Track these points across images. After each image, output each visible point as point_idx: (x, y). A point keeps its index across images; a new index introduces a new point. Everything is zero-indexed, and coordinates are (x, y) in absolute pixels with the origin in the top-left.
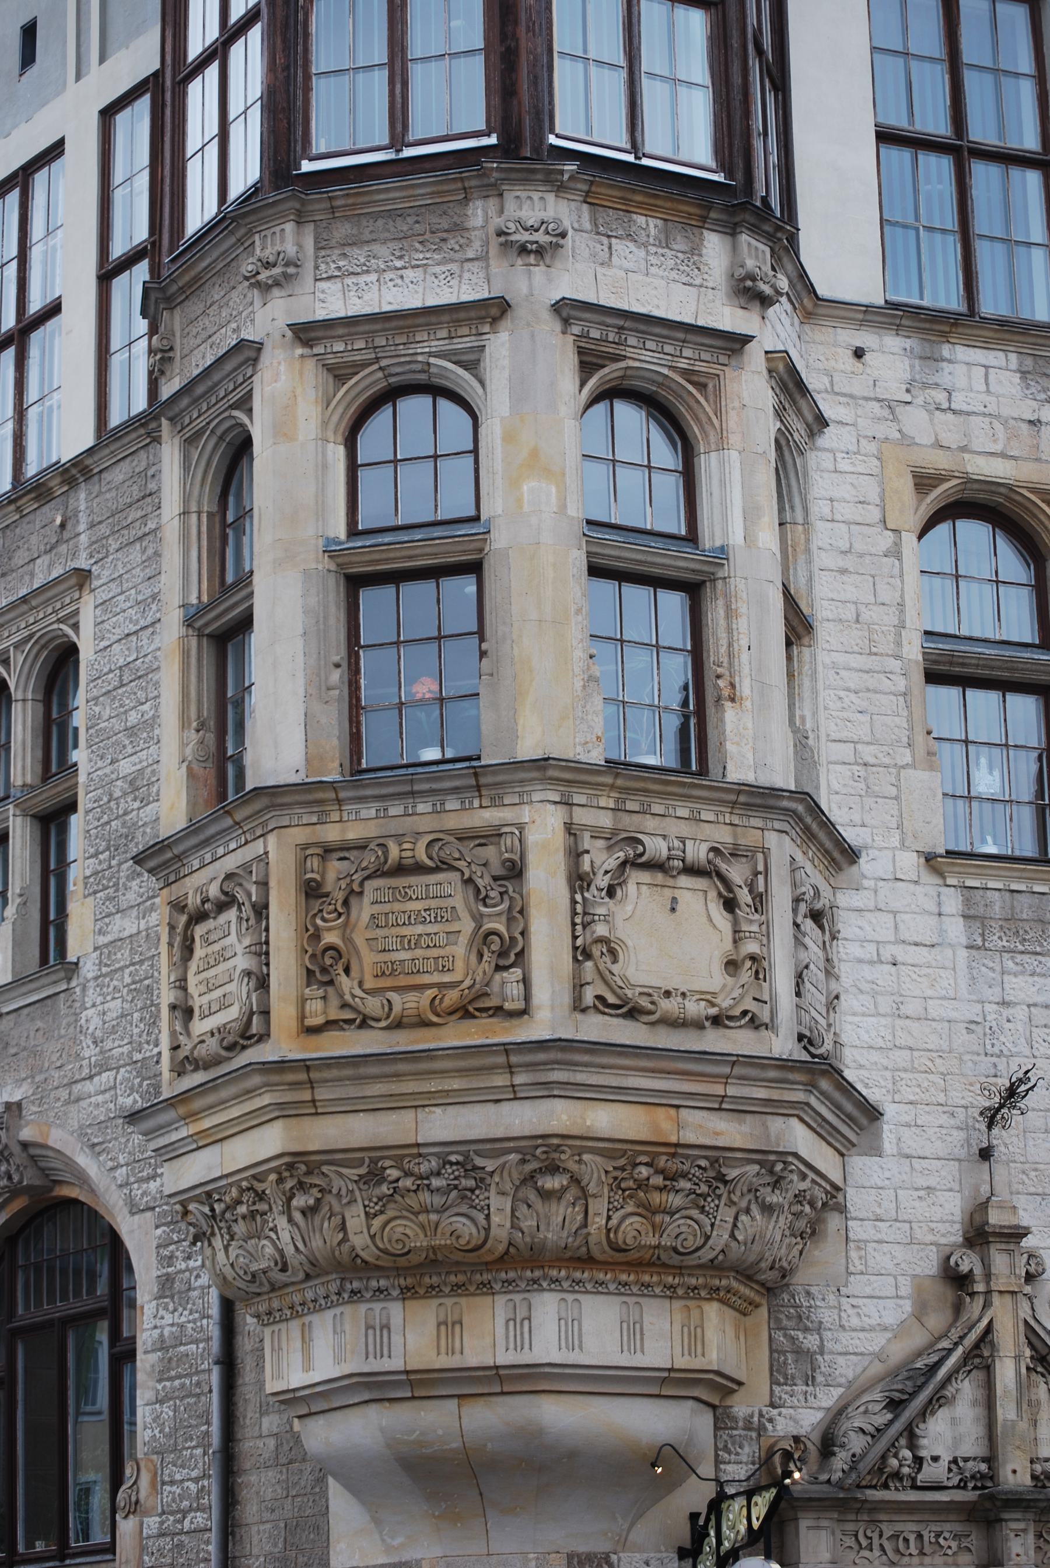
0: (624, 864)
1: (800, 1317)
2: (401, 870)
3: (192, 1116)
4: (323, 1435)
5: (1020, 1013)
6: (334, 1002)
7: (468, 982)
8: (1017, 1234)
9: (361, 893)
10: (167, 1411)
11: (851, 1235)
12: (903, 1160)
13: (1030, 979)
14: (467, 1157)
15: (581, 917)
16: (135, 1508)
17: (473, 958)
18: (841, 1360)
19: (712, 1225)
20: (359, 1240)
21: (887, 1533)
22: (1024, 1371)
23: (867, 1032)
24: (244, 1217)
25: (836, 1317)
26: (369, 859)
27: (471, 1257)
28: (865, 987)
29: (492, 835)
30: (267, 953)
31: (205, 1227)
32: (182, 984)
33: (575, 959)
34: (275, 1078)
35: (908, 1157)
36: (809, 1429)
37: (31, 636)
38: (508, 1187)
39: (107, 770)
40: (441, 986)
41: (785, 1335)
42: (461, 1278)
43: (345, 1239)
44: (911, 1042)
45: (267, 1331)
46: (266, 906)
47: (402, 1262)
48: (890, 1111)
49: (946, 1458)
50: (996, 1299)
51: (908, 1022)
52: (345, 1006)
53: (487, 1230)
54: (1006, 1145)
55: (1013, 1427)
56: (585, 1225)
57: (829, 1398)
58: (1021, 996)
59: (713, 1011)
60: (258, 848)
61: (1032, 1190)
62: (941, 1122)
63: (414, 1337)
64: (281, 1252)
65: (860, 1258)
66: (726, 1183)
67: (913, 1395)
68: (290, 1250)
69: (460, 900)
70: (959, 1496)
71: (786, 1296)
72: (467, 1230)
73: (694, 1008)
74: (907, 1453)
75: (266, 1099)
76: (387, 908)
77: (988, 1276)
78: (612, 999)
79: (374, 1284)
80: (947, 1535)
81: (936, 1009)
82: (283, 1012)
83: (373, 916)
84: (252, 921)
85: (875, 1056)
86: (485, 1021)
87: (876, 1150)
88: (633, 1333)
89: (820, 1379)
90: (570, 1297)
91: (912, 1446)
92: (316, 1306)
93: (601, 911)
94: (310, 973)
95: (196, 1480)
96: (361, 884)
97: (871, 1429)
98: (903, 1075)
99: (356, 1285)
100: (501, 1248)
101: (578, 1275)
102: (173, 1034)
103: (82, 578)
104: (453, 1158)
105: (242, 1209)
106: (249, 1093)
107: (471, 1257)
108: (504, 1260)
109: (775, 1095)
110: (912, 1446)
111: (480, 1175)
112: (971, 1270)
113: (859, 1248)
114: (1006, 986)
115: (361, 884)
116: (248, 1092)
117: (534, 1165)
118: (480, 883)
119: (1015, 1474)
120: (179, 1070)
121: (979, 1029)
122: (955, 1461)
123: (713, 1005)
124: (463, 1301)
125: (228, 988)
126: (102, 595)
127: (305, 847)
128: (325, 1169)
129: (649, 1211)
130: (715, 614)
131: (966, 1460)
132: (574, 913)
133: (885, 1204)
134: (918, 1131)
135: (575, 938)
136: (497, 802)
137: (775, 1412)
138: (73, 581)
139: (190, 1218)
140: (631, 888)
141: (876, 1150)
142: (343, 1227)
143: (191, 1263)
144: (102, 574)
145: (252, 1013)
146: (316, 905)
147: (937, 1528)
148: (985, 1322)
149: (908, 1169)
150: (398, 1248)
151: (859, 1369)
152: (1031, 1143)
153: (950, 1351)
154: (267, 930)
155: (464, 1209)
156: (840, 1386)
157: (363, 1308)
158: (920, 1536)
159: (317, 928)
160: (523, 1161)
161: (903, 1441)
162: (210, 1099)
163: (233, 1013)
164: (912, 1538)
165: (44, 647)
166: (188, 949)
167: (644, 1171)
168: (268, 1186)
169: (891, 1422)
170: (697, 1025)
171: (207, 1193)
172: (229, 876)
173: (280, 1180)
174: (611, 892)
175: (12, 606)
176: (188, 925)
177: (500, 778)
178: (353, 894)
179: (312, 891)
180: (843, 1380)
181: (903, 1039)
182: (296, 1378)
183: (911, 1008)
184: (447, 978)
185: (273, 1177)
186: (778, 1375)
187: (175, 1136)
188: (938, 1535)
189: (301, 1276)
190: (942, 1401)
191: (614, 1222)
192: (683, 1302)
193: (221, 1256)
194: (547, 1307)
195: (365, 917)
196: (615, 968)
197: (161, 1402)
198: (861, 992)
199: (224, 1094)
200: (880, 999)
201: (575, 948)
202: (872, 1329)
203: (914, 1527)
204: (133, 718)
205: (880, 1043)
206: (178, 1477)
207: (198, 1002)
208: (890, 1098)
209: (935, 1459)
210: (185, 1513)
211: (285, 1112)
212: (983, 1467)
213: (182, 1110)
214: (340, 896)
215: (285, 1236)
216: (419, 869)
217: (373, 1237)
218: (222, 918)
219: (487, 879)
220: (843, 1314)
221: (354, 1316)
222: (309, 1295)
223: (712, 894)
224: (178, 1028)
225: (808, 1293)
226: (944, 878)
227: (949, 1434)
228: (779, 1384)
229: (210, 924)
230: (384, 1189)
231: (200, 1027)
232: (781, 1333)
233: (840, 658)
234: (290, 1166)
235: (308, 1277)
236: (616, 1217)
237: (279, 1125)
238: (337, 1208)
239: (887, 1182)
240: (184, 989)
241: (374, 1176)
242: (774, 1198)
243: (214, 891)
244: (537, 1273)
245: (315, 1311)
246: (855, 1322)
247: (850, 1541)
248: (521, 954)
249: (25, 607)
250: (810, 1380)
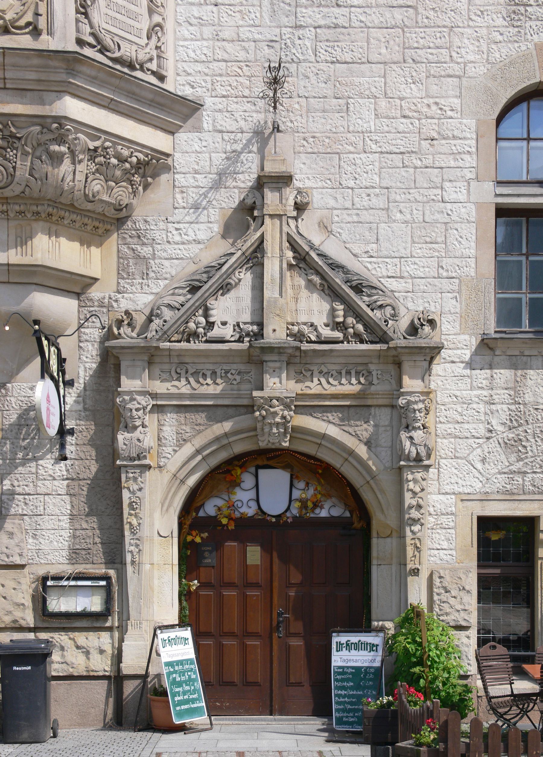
1: (139, 237)
5: (310, 33)
11: (176, 183)
12: (216, 134)
13: (316, 9)
18: (166, 263)
19: (14, 168)
21: (191, 371)
22: (285, 266)
23: (194, 51)
25: (164, 236)
28: (194, 21)
35: (221, 132)
36: (143, 306)
41: (129, 248)
44: (226, 57)
48: (209, 102)
49: (232, 322)
50: (267, 220)
51: (225, 44)
54: (291, 121)
55: (275, 302)
57: (158, 286)
58: (310, 21)
61: (310, 150)
62: (245, 108)
65: (183, 198)
71: (129, 223)
74: (202, 320)
80: (233, 372)
81: (245, 33)
85: (199, 67)
87: (198, 129)
89: (152, 275)
91: (206, 315)
97: (177, 305)
98: (219, 78)
109: (43, 77)
110: (206, 315)
112: (254, 203)
113: (182, 192)
114: (299, 15)
119: (276, 333)
121: (277, 46)
133: (202, 163)
134: (228, 115)
137: (120, 296)
141: (198, 129)
149: (220, 140)
151: (179, 269)
152: (311, 119)
156: (166, 279)
161: (201, 312)
180: (168, 276)
181: (220, 55)
183: (227, 34)
186: (123, 272)
188: (227, 372)
190: (229, 286)
192: (16, 222)
198: (191, 24)
200: (204, 29)
202: (189, 242)
203: (211, 367)
205: (204, 58)
208: (209, 94)
209: (224, 324)
212: (255, 328)
220: (169, 234)
225: (146, 221)
228: (123, 278)
232: (125, 247)
239: (204, 149)
246: (177, 238)
250: (145, 275)
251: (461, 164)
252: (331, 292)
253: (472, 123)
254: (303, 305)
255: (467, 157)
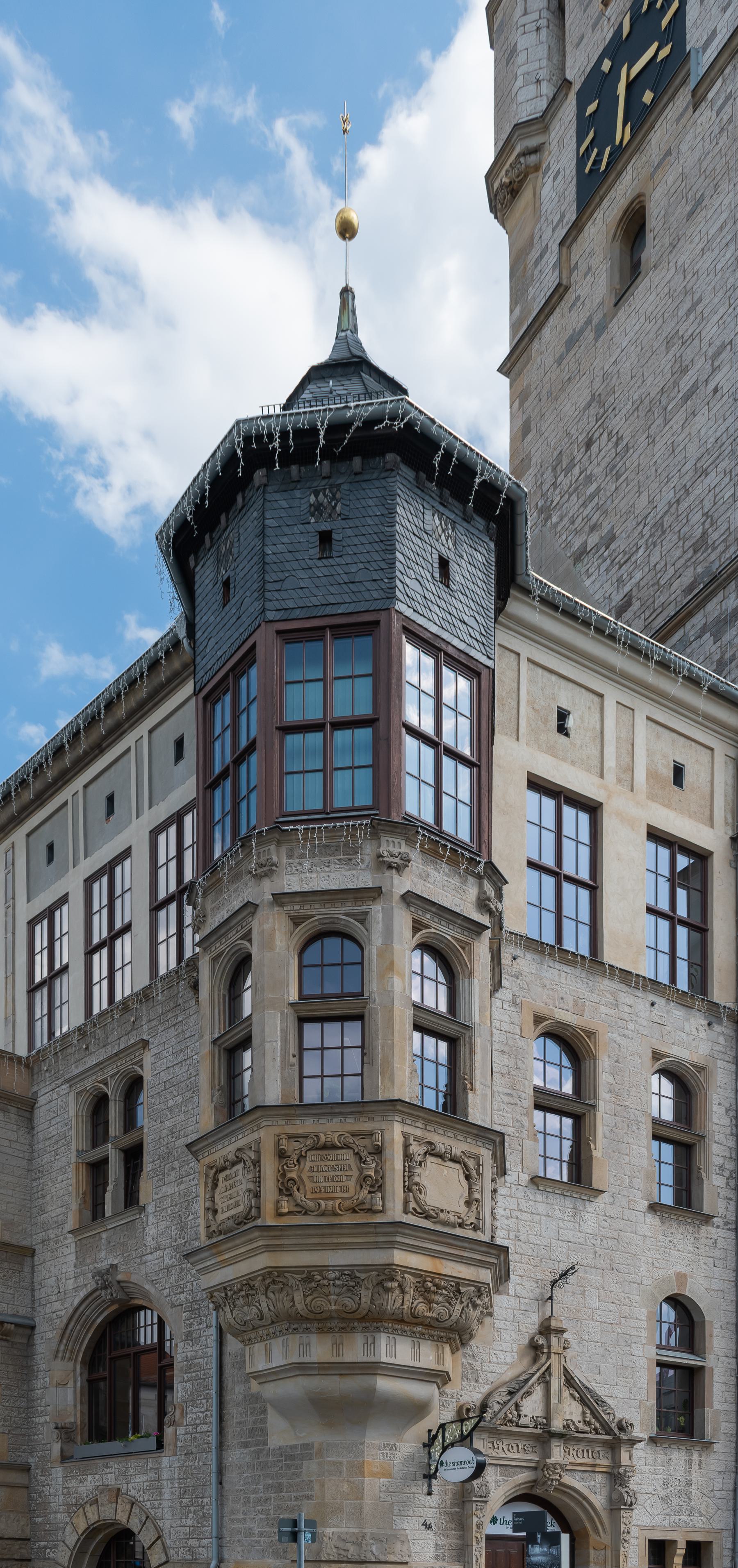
0: (426, 1153)
2: (325, 1147)
3: (220, 1253)
4: (271, 1390)
6: (292, 1203)
7: (356, 1197)
8: (561, 1331)
9: (305, 1157)
10: (189, 1385)
14: (352, 1271)
15: (409, 1173)
16: (173, 1423)
17: (358, 1187)
20: (300, 1307)
24: (243, 1297)
26: (309, 1142)
27: (350, 1316)
29: (371, 1134)
30: (259, 1182)
31: (221, 1302)
32: (212, 1199)
33: (404, 1191)
34: (265, 1234)
37: (118, 1072)
38: (371, 1286)
39: (159, 1126)
40: (343, 1198)
42: (344, 1325)
43: (294, 1305)
45: (247, 1348)
46: (259, 1161)
47: (318, 1316)
52: (297, 1205)
53: (359, 1304)
56: (402, 1305)
59: (460, 1221)
60: (255, 1136)
63: (319, 1350)
64: (261, 1311)
66: (460, 1293)
67: (519, 1390)
68: (266, 1310)
69: (352, 1161)
70: (534, 1431)
72: (350, 1304)
73: (452, 1218)
75: (260, 1243)
76: (317, 1163)
77: (549, 1347)
78: (419, 1210)
79: (304, 1326)
82: (268, 1207)
83: (311, 1167)
84: (252, 1168)
86: (362, 1214)
88: (416, 1355)
90: (391, 1336)
92: (275, 1336)
93: (417, 1171)
94: (280, 1190)
95: (203, 1412)
96: (306, 1153)
99: (296, 1326)
100: (365, 1312)
101: (396, 1326)
102: (207, 1220)
103: (145, 1044)
104: (346, 1272)
105: (243, 1293)
106: (251, 1241)
107: (350, 1316)
108: (363, 1319)
111: (358, 1280)
115: (306, 1153)
116: (251, 1240)
117: (383, 1277)
118: (362, 1154)
119: (557, 1425)
120: (209, 1236)
122: (533, 1417)
123: (459, 1218)
124: (344, 1335)
125: (237, 1199)
126: (154, 1051)
127: (278, 1135)
128: (286, 1274)
129: (429, 1302)
130: (463, 1052)
131: (537, 1417)
132: (404, 1171)
135: (404, 1182)
136: (371, 1119)
138: (141, 1045)
139: (214, 1299)
140: (428, 1163)
142: (293, 1300)
143: (201, 1326)
144: (154, 1042)
145: (251, 1207)
146: (284, 1161)
147: (525, 1442)
148: (548, 1364)
150: (318, 1310)
153: (533, 1375)
154: (259, 1171)
155: (349, 1294)
157: (298, 1336)
158: (517, 1446)
159: (284, 1170)
160: (378, 1275)
162: (230, 1245)
163: (241, 1208)
164: (515, 1446)
165: (125, 1077)
166: (215, 1185)
167: (430, 1284)
168: (256, 1283)
169: (509, 1401)
170: (453, 1226)
171: (224, 1287)
172: (239, 1150)
173: (264, 1280)
174: (420, 1164)
175: (110, 1058)
176: (216, 1173)
177: (373, 1108)
178: (301, 1157)
179: (281, 1155)
182: (261, 1365)
184: (345, 1195)
185: (260, 1278)
187: (209, 1263)
189: (270, 1322)
191: (415, 1305)
193: (229, 1315)
194: (383, 1341)
195: (307, 1167)
196: (421, 1197)
197: (186, 1382)
199: (238, 1242)
201: (404, 1186)
204: (171, 1103)
206: (194, 1411)
207: (219, 1206)
209: (525, 1416)
210: (197, 1425)
211: (268, 1248)
212: (544, 1421)
213: (214, 1251)
214: (296, 1157)
215: (264, 1304)
216: (334, 1147)
217: (306, 1305)
218: (235, 1168)
219: (366, 1153)
221: (294, 1340)
222: (272, 1331)
223: (461, 1172)
224: (211, 1218)
226: (538, 1187)
227: (532, 1406)
229: (228, 1172)
230: (313, 1285)
231: (221, 1217)
233: (501, 1089)
234: (270, 1273)
235: (273, 1322)
236: (416, 1303)
237: (266, 1254)
238: (290, 1291)
240: (213, 1201)
241: (309, 1279)
242: (479, 1302)
243: (231, 1157)
244: (380, 1324)
245: (274, 1338)
247: (491, 1445)
248: (380, 1187)
249: (116, 1058)
251: (640, 1334)
252: (583, 1401)
253: (644, 1311)
254: (567, 1409)
255: (642, 1330)
